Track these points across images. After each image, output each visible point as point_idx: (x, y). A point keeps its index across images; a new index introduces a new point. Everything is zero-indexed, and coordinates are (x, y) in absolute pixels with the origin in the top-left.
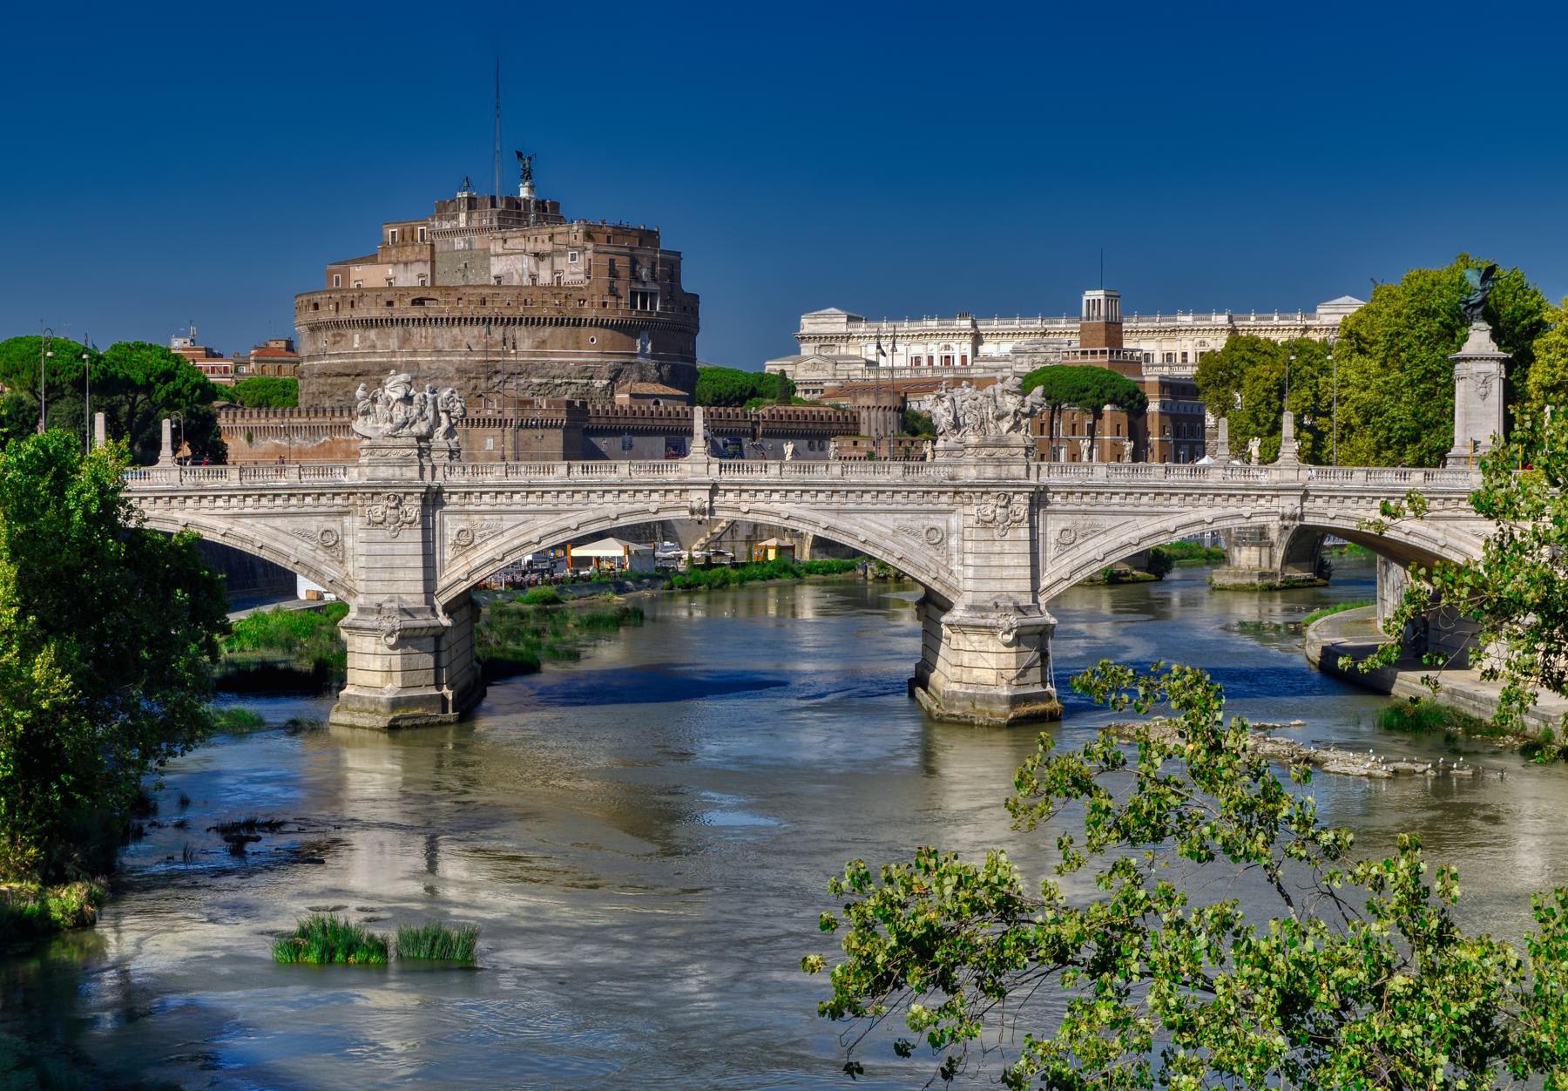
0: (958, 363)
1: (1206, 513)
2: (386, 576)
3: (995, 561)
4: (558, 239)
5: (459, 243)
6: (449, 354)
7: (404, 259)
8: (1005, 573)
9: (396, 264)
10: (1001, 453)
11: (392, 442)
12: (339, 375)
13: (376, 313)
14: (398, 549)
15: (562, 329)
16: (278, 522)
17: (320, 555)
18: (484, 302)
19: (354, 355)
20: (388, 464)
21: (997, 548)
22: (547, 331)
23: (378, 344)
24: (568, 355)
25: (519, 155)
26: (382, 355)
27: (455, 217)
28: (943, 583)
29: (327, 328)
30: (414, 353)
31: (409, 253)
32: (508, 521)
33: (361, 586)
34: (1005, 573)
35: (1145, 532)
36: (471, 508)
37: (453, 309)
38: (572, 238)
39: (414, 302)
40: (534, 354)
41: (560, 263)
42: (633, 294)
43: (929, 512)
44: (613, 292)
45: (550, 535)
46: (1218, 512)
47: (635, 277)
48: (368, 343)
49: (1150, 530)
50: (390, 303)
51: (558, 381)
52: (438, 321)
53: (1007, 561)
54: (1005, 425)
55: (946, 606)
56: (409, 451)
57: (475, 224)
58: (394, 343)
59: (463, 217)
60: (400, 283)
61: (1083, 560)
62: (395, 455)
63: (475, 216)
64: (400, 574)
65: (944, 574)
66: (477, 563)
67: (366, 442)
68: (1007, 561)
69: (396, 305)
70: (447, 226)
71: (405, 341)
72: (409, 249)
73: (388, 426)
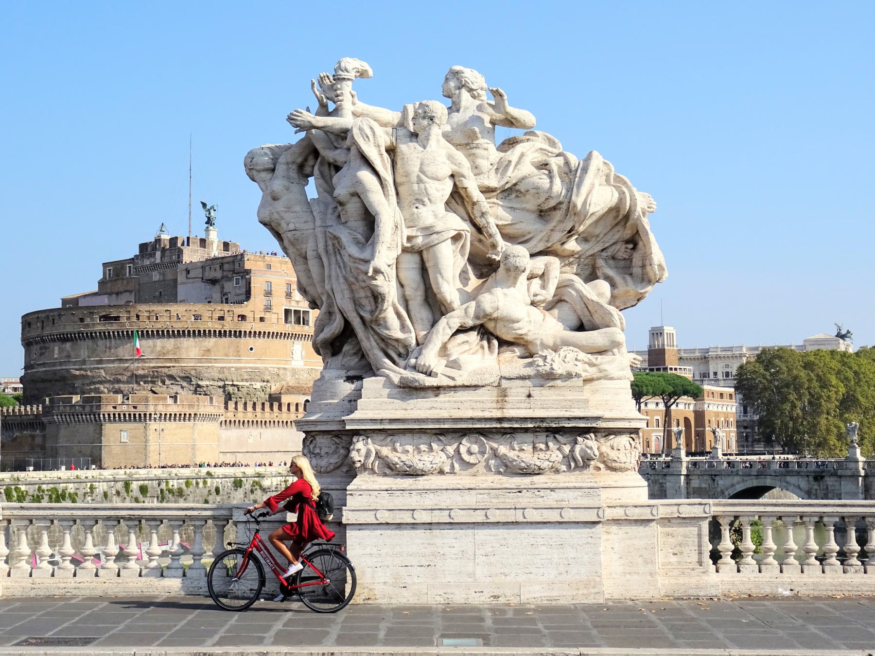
4: (226, 267)
5: (156, 276)
7: (116, 290)
9: (110, 294)
12: (43, 381)
13: (69, 329)
15: (224, 339)
19: (54, 364)
22: (211, 342)
23: (72, 354)
24: (229, 361)
25: (204, 205)
27: (153, 255)
29: (37, 343)
31: (120, 286)
41: (229, 286)
42: (287, 312)
48: (65, 354)
50: (82, 320)
57: (166, 260)
59: (158, 254)
69: (88, 321)
70: (147, 262)
71: (93, 352)
72: (120, 282)
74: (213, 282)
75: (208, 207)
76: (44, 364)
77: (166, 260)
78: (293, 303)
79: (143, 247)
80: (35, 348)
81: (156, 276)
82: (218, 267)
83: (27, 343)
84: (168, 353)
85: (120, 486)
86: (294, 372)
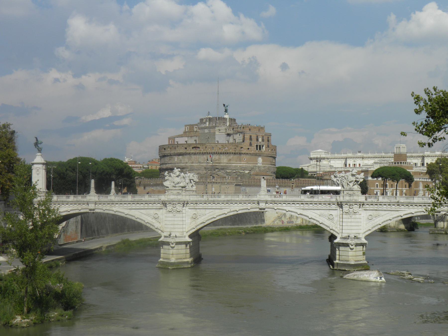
0: (358, 166)
1: (413, 211)
2: (172, 226)
3: (349, 224)
4: (235, 129)
5: (206, 131)
6: (202, 163)
8: (352, 228)
10: (350, 192)
11: (174, 188)
14: (176, 219)
16: (142, 211)
17: (154, 221)
20: (173, 195)
21: (350, 220)
22: (231, 156)
25: (224, 105)
27: (205, 123)
28: (334, 230)
30: (192, 163)
31: (192, 134)
32: (208, 211)
33: (165, 230)
34: (352, 228)
35: (394, 216)
36: (197, 207)
37: (204, 150)
38: (239, 129)
39: (193, 148)
40: (227, 163)
42: (257, 146)
43: (329, 210)
44: (251, 145)
45: (219, 215)
46: (416, 210)
47: (257, 140)
49: (396, 216)
50: (186, 148)
51: (234, 171)
52: (199, 154)
53: (353, 224)
54: (351, 184)
55: (335, 238)
56: (179, 191)
57: (211, 125)
58: (186, 160)
59: (208, 123)
60: (188, 142)
61: (376, 224)
62: (175, 192)
63: (211, 123)
64: (176, 226)
65: (334, 228)
66: (199, 223)
67: (167, 189)
68: (353, 224)
69: (188, 148)
70: (203, 126)
73: (173, 184)
78: (259, 143)
79: (201, 120)
82: (232, 129)
84: (216, 160)
86: (259, 167)
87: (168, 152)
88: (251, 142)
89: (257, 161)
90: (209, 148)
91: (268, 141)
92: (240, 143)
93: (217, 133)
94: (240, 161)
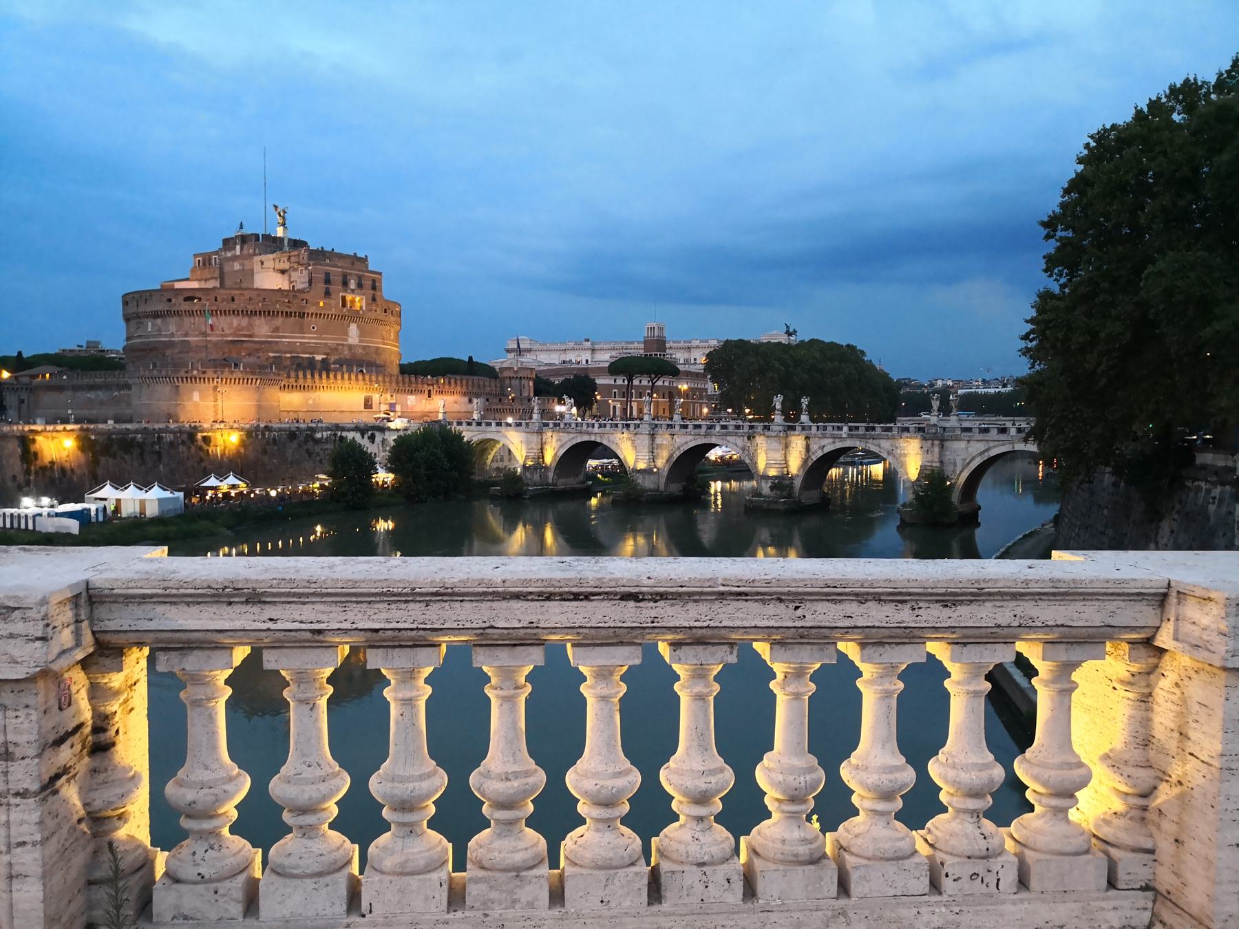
4: (293, 259)
5: (237, 266)
18: (233, 300)
22: (279, 321)
25: (276, 207)
26: (165, 336)
30: (186, 335)
39: (186, 299)
50: (170, 300)
58: (172, 328)
59: (238, 247)
71: (179, 327)
74: (283, 272)
75: (280, 209)
76: (140, 337)
77: (245, 252)
79: (226, 241)
80: (133, 323)
81: (237, 266)
83: (127, 319)
85: (185, 437)
86: (351, 347)
87: (132, 309)
88: (327, 289)
89: (347, 334)
90: (223, 300)
91: (374, 288)
92: (302, 291)
93: (257, 267)
94: (302, 331)
